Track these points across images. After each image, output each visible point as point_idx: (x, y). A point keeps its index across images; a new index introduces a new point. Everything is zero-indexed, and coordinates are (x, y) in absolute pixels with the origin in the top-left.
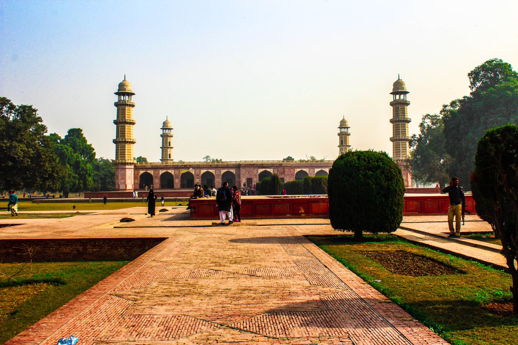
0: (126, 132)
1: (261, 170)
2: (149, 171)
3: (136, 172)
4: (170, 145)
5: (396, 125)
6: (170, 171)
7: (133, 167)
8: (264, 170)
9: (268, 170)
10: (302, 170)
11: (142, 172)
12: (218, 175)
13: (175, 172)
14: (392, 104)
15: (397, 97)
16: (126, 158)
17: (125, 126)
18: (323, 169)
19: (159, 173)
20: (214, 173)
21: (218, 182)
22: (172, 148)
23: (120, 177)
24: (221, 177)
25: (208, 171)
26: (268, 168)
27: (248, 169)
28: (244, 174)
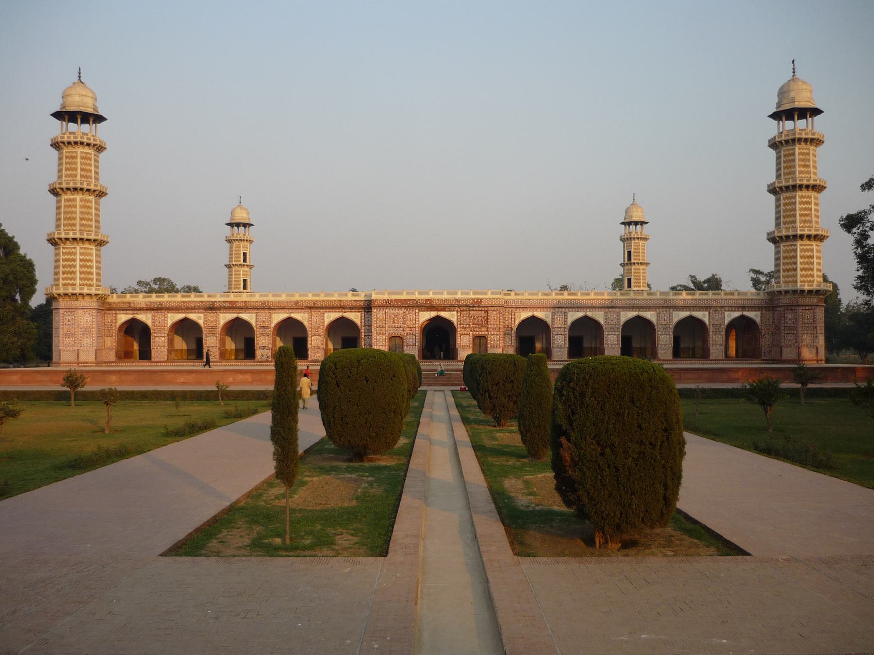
0: (78, 216)
1: (425, 316)
2: (142, 317)
3: (109, 317)
4: (245, 261)
5: (787, 198)
6: (193, 316)
7: (94, 303)
8: (433, 314)
9: (444, 314)
10: (533, 317)
11: (123, 318)
12: (318, 325)
13: (206, 317)
14: (774, 145)
15: (789, 125)
16: (78, 282)
17: (74, 200)
18: (589, 314)
19: (166, 320)
20: (306, 323)
21: (318, 346)
22: (250, 267)
23: (62, 332)
24: (323, 332)
25: (290, 318)
26: (443, 309)
27: (391, 312)
28: (382, 326)
